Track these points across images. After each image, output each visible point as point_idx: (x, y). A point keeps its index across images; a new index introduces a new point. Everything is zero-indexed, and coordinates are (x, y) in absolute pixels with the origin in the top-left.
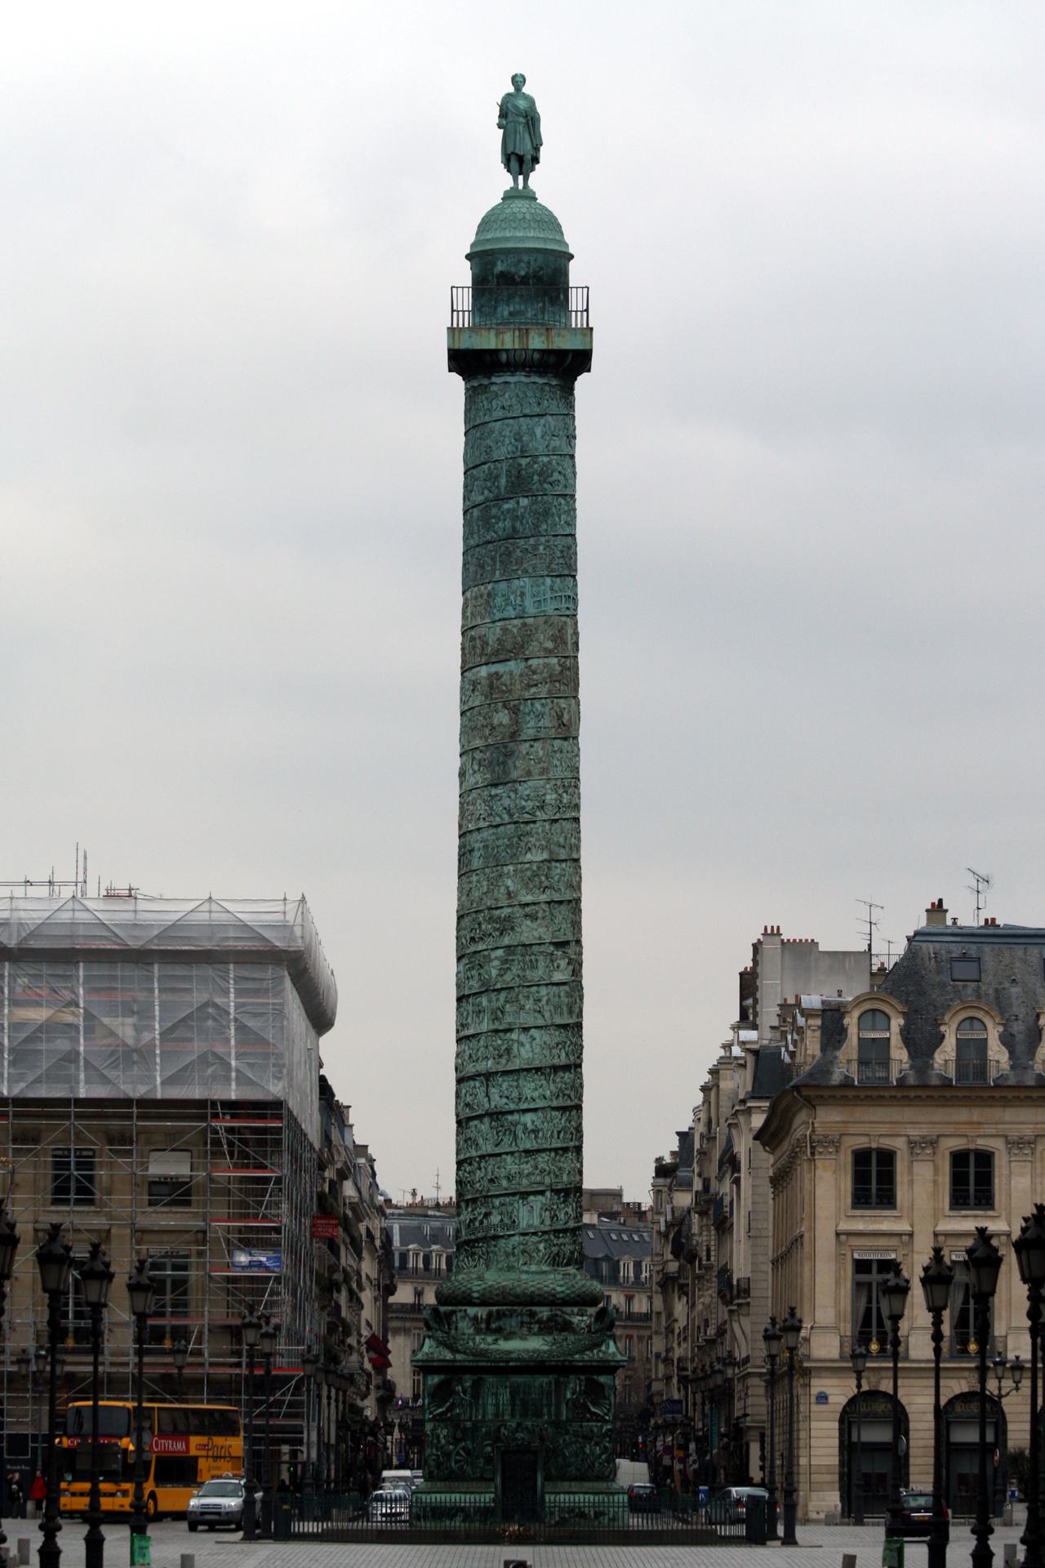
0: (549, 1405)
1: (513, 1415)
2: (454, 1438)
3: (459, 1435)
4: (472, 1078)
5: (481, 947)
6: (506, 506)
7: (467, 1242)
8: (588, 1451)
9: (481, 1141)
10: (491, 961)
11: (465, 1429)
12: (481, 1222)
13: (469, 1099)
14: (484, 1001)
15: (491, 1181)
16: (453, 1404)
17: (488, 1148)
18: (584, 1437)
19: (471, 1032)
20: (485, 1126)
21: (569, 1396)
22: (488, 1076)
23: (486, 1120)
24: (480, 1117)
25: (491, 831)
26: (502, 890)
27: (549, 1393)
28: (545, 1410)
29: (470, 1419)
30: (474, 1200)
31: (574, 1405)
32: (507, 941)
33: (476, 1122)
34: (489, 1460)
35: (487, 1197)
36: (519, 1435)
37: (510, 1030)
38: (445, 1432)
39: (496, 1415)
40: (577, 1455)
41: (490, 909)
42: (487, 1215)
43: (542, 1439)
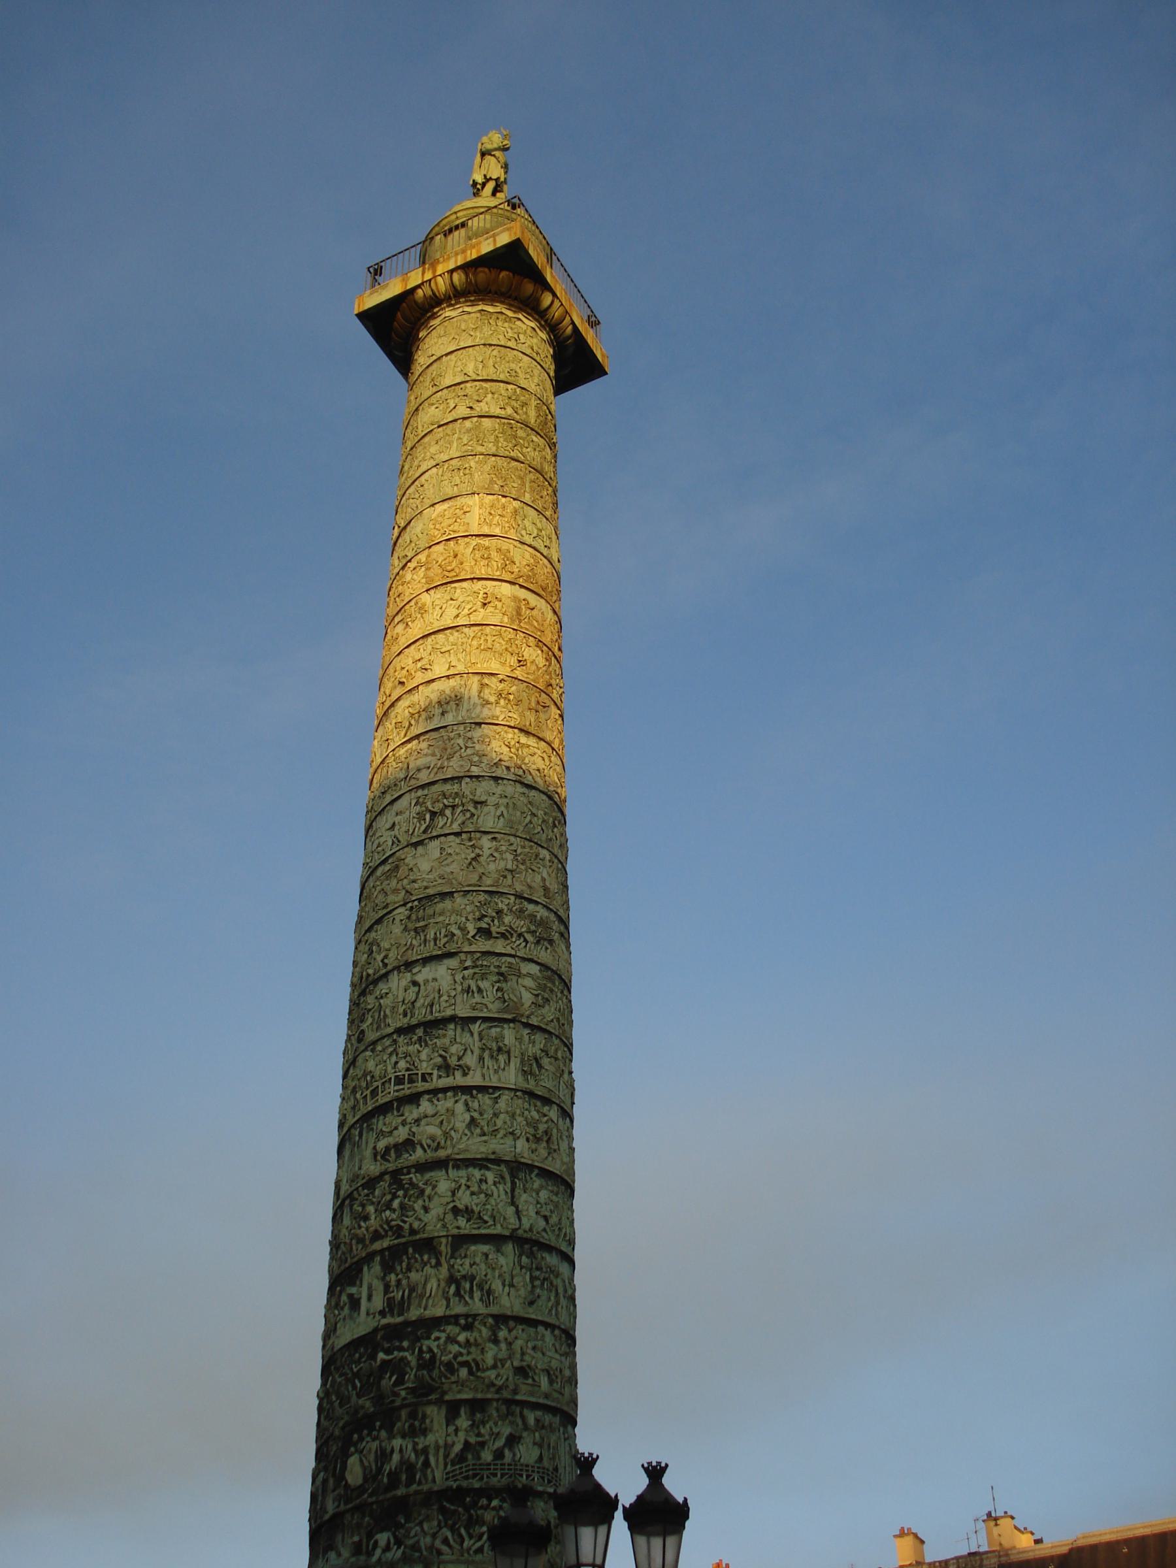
4: (481, 1163)
5: (499, 946)
6: (535, 439)
7: (457, 1495)
9: (497, 1285)
10: (519, 975)
12: (499, 1454)
13: (464, 1199)
14: (509, 1035)
15: (522, 1371)
17: (510, 1302)
19: (474, 1079)
20: (507, 1259)
22: (517, 1168)
23: (509, 1248)
24: (496, 1240)
25: (520, 789)
26: (538, 878)
30: (477, 1406)
32: (544, 956)
33: (485, 1248)
35: (509, 1402)
37: (547, 1101)
41: (519, 896)
42: (512, 1441)
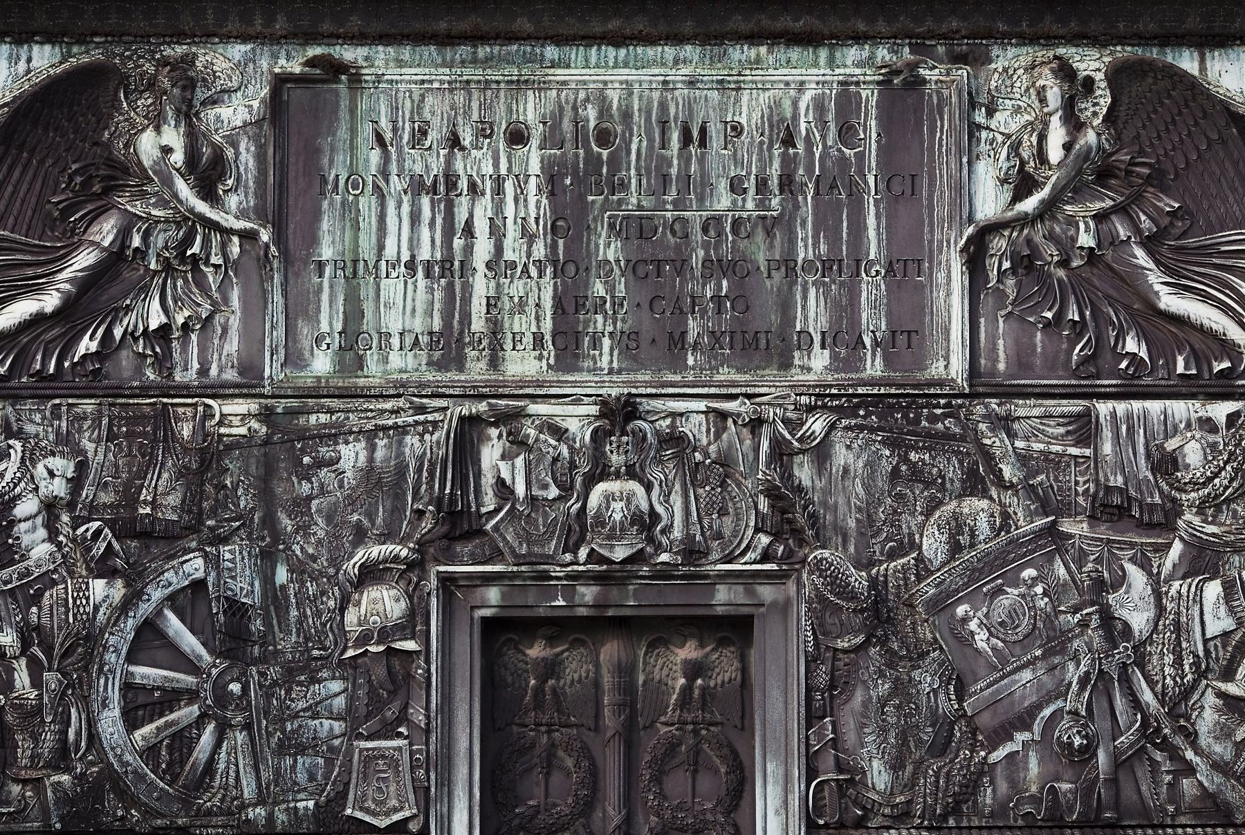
0: (841, 267)
1: (568, 344)
2: (127, 526)
3: (163, 494)
8: (1139, 621)
11: (210, 455)
16: (117, 260)
18: (1111, 509)
21: (989, 201)
27: (838, 185)
28: (813, 313)
29: (248, 381)
31: (1013, 265)
34: (386, 686)
36: (611, 497)
38: (54, 472)
39: (448, 346)
40: (1056, 644)
43: (790, 520)
